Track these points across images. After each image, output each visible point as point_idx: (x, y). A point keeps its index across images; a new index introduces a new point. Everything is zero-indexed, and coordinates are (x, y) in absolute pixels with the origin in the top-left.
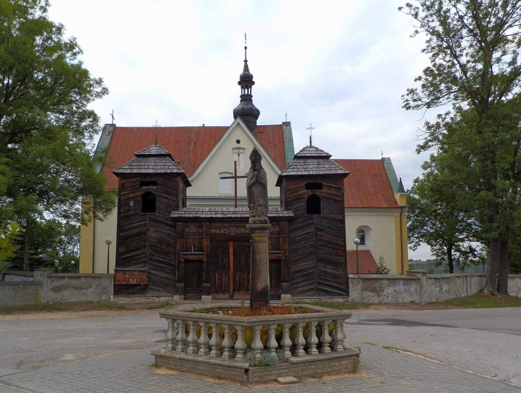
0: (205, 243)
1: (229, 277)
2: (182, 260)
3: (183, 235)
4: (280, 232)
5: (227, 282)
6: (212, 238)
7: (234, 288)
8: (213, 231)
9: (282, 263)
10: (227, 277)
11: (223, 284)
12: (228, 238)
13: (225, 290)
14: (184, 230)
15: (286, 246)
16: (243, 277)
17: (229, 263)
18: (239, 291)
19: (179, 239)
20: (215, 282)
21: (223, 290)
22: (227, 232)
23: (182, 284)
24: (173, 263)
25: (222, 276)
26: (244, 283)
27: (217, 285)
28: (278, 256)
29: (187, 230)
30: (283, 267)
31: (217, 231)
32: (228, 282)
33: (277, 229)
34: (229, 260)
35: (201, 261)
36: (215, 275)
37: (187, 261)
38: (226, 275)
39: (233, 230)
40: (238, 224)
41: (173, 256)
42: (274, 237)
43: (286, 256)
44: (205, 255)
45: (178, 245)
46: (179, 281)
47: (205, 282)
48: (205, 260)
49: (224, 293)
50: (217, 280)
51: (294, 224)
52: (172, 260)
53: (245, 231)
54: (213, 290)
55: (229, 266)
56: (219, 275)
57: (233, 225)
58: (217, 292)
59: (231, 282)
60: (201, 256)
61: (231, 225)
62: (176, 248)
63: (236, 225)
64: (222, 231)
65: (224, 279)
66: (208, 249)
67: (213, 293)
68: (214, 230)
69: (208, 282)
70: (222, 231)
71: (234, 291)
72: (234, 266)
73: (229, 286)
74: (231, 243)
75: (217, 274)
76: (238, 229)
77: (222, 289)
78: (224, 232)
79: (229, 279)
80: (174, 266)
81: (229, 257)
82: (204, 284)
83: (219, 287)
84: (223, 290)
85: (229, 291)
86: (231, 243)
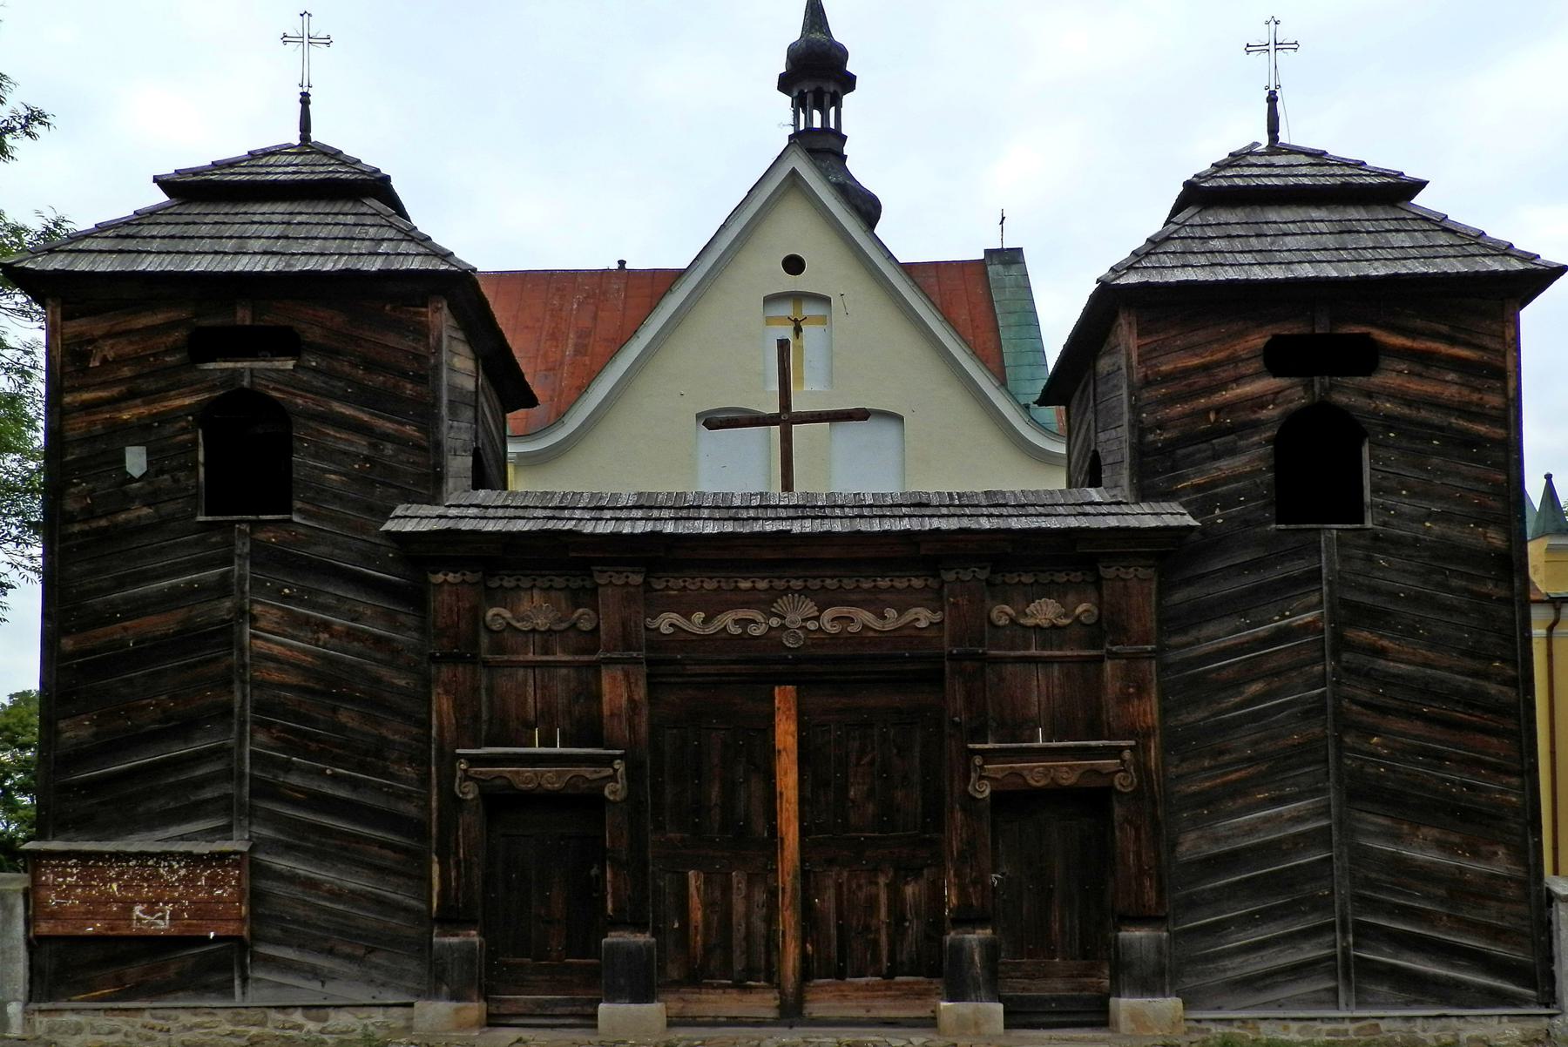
1: (773, 894)
2: (470, 792)
5: (760, 926)
9: (1118, 812)
10: (760, 896)
12: (764, 666)
14: (476, 614)
15: (1149, 710)
16: (862, 895)
17: (771, 814)
19: (445, 672)
24: (410, 809)
25: (727, 889)
26: (867, 928)
28: (1096, 772)
30: (1124, 838)
38: (750, 883)
39: (794, 619)
42: (1061, 661)
43: (1142, 768)
44: (619, 765)
45: (442, 704)
47: (616, 924)
48: (615, 791)
50: (697, 915)
52: (408, 796)
53: (876, 624)
55: (773, 830)
57: (797, 584)
60: (588, 772)
63: (815, 584)
64: (727, 621)
65: (739, 906)
66: (633, 728)
69: (640, 927)
70: (727, 621)
73: (773, 944)
74: (784, 699)
76: (829, 614)
78: (735, 630)
81: (770, 777)
83: (708, 950)
86: (784, 699)
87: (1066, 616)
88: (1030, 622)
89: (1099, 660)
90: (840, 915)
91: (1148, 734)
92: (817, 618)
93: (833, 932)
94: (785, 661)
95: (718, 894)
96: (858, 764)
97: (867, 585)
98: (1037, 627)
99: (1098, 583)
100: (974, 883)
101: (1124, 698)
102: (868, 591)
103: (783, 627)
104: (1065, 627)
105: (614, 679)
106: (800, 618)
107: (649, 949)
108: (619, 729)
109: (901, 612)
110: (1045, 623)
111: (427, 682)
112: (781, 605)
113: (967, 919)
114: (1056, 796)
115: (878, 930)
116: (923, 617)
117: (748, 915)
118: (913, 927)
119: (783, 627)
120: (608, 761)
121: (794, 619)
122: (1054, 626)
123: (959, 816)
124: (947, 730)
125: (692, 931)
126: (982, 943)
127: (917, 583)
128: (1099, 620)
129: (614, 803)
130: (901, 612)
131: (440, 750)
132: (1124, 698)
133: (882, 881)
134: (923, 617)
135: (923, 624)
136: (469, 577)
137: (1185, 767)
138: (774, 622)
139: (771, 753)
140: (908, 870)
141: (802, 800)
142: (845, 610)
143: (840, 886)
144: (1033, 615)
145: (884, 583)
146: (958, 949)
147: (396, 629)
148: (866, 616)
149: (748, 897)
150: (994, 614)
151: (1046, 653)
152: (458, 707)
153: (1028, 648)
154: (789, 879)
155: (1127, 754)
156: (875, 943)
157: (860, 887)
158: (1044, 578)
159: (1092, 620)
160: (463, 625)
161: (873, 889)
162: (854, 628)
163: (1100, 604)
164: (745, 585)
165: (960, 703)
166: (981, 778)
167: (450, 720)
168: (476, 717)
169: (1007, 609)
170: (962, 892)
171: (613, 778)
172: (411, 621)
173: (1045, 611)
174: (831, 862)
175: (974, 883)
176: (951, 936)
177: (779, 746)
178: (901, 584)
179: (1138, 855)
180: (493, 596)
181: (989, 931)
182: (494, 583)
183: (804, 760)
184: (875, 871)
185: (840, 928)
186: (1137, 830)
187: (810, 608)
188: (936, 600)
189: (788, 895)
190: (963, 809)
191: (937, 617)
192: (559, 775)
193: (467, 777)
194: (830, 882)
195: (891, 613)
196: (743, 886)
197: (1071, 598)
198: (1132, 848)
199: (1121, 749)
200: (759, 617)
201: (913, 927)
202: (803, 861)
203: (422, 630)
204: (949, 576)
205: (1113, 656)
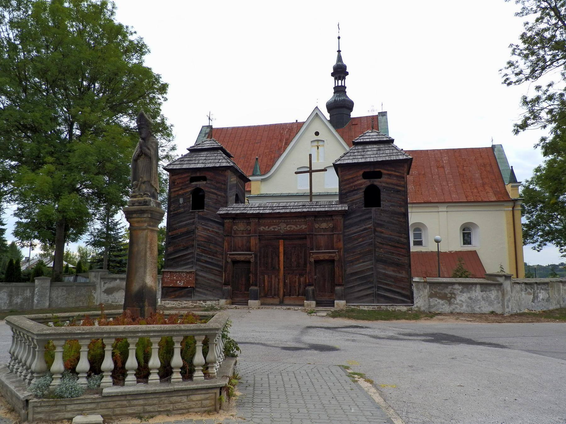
0: (254, 241)
2: (229, 260)
3: (231, 232)
4: (334, 229)
5: (277, 286)
6: (261, 237)
8: (262, 228)
10: (277, 280)
11: (273, 287)
12: (278, 237)
13: (275, 295)
14: (232, 228)
15: (341, 244)
17: (279, 264)
18: (290, 295)
19: (226, 238)
20: (264, 286)
21: (273, 293)
23: (229, 287)
24: (220, 263)
25: (271, 278)
27: (266, 288)
29: (235, 227)
31: (266, 229)
32: (278, 285)
33: (331, 225)
34: (279, 261)
35: (249, 262)
36: (264, 278)
37: (235, 262)
39: (282, 227)
40: (289, 221)
41: (221, 256)
42: (327, 235)
44: (253, 255)
45: (226, 244)
46: (226, 284)
47: (252, 285)
48: (252, 260)
49: (273, 297)
50: (266, 284)
51: (349, 219)
52: (220, 261)
54: (262, 294)
55: (279, 267)
56: (268, 277)
57: (283, 221)
58: (266, 296)
59: (281, 285)
60: (248, 257)
62: (223, 248)
63: (286, 221)
64: (272, 228)
67: (263, 297)
68: (263, 227)
69: (256, 285)
70: (272, 228)
71: (284, 295)
72: (284, 268)
75: (266, 277)
76: (288, 226)
78: (273, 230)
79: (279, 282)
80: (221, 267)
82: (252, 288)
84: (273, 293)
97: (294, 221)
106: (283, 228)
108: (253, 248)
111: (224, 240)
112: (280, 225)
116: (304, 227)
118: (302, 287)
133: (297, 277)
134: (304, 227)
139: (279, 252)
140: (301, 275)
145: (297, 220)
148: (294, 227)
152: (228, 245)
158: (324, 219)
168: (231, 246)
173: (324, 225)
174: (289, 274)
178: (300, 220)
180: (234, 224)
187: (285, 225)
191: (306, 227)
195: (298, 226)
201: (302, 287)
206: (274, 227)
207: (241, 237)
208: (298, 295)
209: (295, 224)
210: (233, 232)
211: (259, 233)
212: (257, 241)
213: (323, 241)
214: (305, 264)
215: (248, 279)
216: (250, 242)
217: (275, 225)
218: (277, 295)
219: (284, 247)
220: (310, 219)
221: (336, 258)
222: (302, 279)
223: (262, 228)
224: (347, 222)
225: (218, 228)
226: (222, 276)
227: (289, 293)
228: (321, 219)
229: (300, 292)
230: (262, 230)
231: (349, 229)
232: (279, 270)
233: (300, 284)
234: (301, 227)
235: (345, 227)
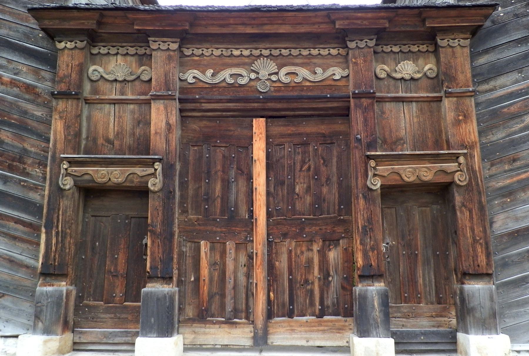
0: (161, 117)
1: (250, 257)
2: (68, 183)
3: (80, 86)
4: (441, 81)
5: (242, 279)
6: (189, 102)
7: (269, 302)
8: (190, 76)
9: (458, 199)
10: (243, 259)
11: (230, 285)
12: (247, 105)
13: (236, 312)
14: (82, 69)
15: (471, 130)
16: (304, 258)
17: (251, 203)
18: (290, 315)
19: (61, 105)
20: (198, 279)
21: (229, 308)
22: (243, 81)
23: (63, 287)
24: (34, 196)
25: (223, 253)
26: (306, 281)
27: (205, 289)
28: (444, 172)
29: (95, 70)
30: (463, 217)
31: (207, 77)
32: (249, 275)
33: (430, 67)
34: (250, 192)
35: (141, 193)
36: (198, 250)
37: (90, 192)
38: (237, 249)
39: (264, 74)
40: (285, 52)
41: (37, 171)
42: (417, 100)
43: (471, 170)
44: (158, 166)
45: (58, 126)
46: (49, 273)
47: (152, 278)
48: (155, 184)
49: (229, 322)
50: (205, 272)
51: (487, 51)
52: (35, 188)
53: (311, 78)
54: (190, 312)
55: (251, 213)
56: (212, 249)
57: (266, 52)
58: (203, 317)
59: (260, 275)
60: (139, 171)
61: (256, 52)
62: (48, 140)
63: (276, 52)
64: (226, 75)
65: (230, 266)
66: (168, 141)
67: (191, 321)
68: (196, 73)
69: (167, 279)
70: (226, 75)
71: (270, 315)
72: (269, 215)
73: (250, 294)
74: (259, 125)
75: (204, 246)
76: (284, 71)
77: (223, 306)
78: (230, 81)
79: (250, 266)
80: (34, 208)
81: (250, 178)
82: (154, 288)
83: (211, 297)
84: (229, 308)
85: (248, 315)
86: (259, 125)
87: (419, 72)
88: (398, 76)
89: (439, 100)
90: (290, 273)
91: (472, 147)
92: (277, 73)
93: (286, 284)
94: (257, 100)
95: (218, 257)
96: (301, 170)
97: (305, 52)
98: (402, 79)
99: (436, 52)
100: (372, 249)
101: (457, 123)
102: (306, 57)
103: (258, 79)
104: (420, 78)
105: (158, 109)
106: (267, 72)
107: (172, 298)
108: (158, 143)
109: (324, 70)
110: (407, 77)
111: (51, 110)
112: (258, 64)
113: (370, 275)
114: (422, 189)
115: (313, 283)
116: (338, 72)
117: (235, 272)
118: (335, 281)
119: (258, 79)
120: (151, 163)
121: (264, 74)
122: (412, 79)
123: (362, 202)
124: (353, 144)
125: (202, 282)
126: (378, 292)
127: (334, 52)
128: (437, 76)
129: (154, 192)
130: (324, 70)
131: (54, 157)
132: (457, 123)
133: (316, 247)
134: (338, 72)
135: (337, 77)
136: (80, 44)
137: (494, 170)
138: (253, 76)
139: (250, 161)
140: (331, 241)
141: (268, 194)
142: (292, 69)
143: (290, 251)
144: (400, 72)
145: (315, 52)
146: (363, 297)
147: (38, 80)
148: (304, 72)
149: (236, 260)
150: (378, 71)
151: (409, 95)
152: (67, 127)
153: (398, 92)
154: (260, 247)
155: (462, 159)
156: (312, 292)
157: (302, 253)
158: (405, 49)
159: (434, 75)
160: (74, 75)
161: (310, 254)
162: (298, 80)
163: (438, 62)
164: (236, 53)
165: (360, 126)
166: (375, 175)
167: (61, 136)
168: (78, 134)
169: (386, 67)
170: (365, 256)
171: (153, 175)
172: (47, 75)
173: (407, 68)
174: (285, 236)
175: (372, 249)
176: (359, 288)
177: (255, 158)
178: (324, 52)
179: (472, 230)
180: (93, 58)
181: (382, 284)
182: (95, 51)
183: (269, 167)
184: (311, 241)
185: (290, 281)
186: (471, 211)
187: (273, 67)
188: (345, 61)
189: (259, 258)
190: (365, 197)
191: (345, 73)
192: (122, 173)
193: (68, 174)
194: (284, 250)
195: (319, 70)
196: (233, 251)
197: (421, 61)
198: (468, 224)
199: (457, 156)
200: (244, 72)
201: (335, 281)
202: (268, 235)
203: (53, 81)
204: (352, 45)
205: (449, 95)
206: (235, 71)
207: (114, 102)
208: (321, 315)
209: (308, 62)
210: (87, 87)
211: (182, 90)
212: (174, 118)
213: (404, 120)
214: (346, 201)
215: (138, 254)
216: (148, 124)
217: (237, 65)
218: (241, 313)
219: (268, 144)
220: (362, 44)
221: (461, 179)
222: (333, 255)
223: (190, 76)
224: (482, 60)
225: (36, 72)
226: (38, 244)
227: (286, 306)
228: (396, 49)
229: (329, 302)
230: (191, 80)
231: (492, 84)
232: (250, 222)
233: (325, 274)
234: (329, 72)
235: (482, 76)
